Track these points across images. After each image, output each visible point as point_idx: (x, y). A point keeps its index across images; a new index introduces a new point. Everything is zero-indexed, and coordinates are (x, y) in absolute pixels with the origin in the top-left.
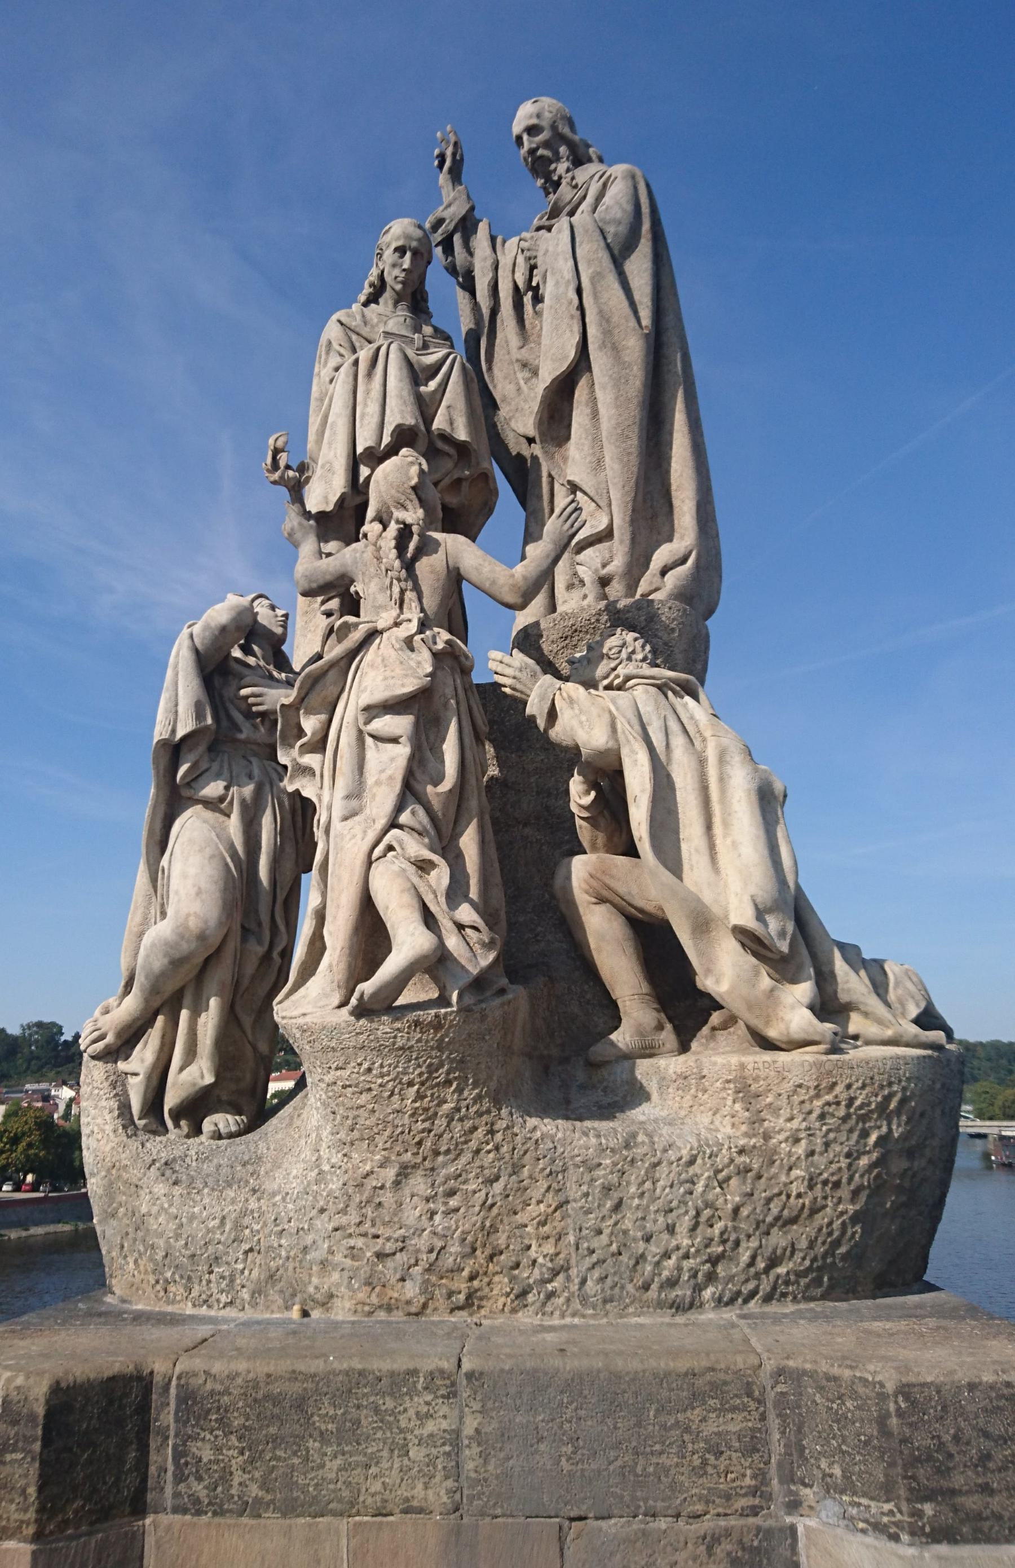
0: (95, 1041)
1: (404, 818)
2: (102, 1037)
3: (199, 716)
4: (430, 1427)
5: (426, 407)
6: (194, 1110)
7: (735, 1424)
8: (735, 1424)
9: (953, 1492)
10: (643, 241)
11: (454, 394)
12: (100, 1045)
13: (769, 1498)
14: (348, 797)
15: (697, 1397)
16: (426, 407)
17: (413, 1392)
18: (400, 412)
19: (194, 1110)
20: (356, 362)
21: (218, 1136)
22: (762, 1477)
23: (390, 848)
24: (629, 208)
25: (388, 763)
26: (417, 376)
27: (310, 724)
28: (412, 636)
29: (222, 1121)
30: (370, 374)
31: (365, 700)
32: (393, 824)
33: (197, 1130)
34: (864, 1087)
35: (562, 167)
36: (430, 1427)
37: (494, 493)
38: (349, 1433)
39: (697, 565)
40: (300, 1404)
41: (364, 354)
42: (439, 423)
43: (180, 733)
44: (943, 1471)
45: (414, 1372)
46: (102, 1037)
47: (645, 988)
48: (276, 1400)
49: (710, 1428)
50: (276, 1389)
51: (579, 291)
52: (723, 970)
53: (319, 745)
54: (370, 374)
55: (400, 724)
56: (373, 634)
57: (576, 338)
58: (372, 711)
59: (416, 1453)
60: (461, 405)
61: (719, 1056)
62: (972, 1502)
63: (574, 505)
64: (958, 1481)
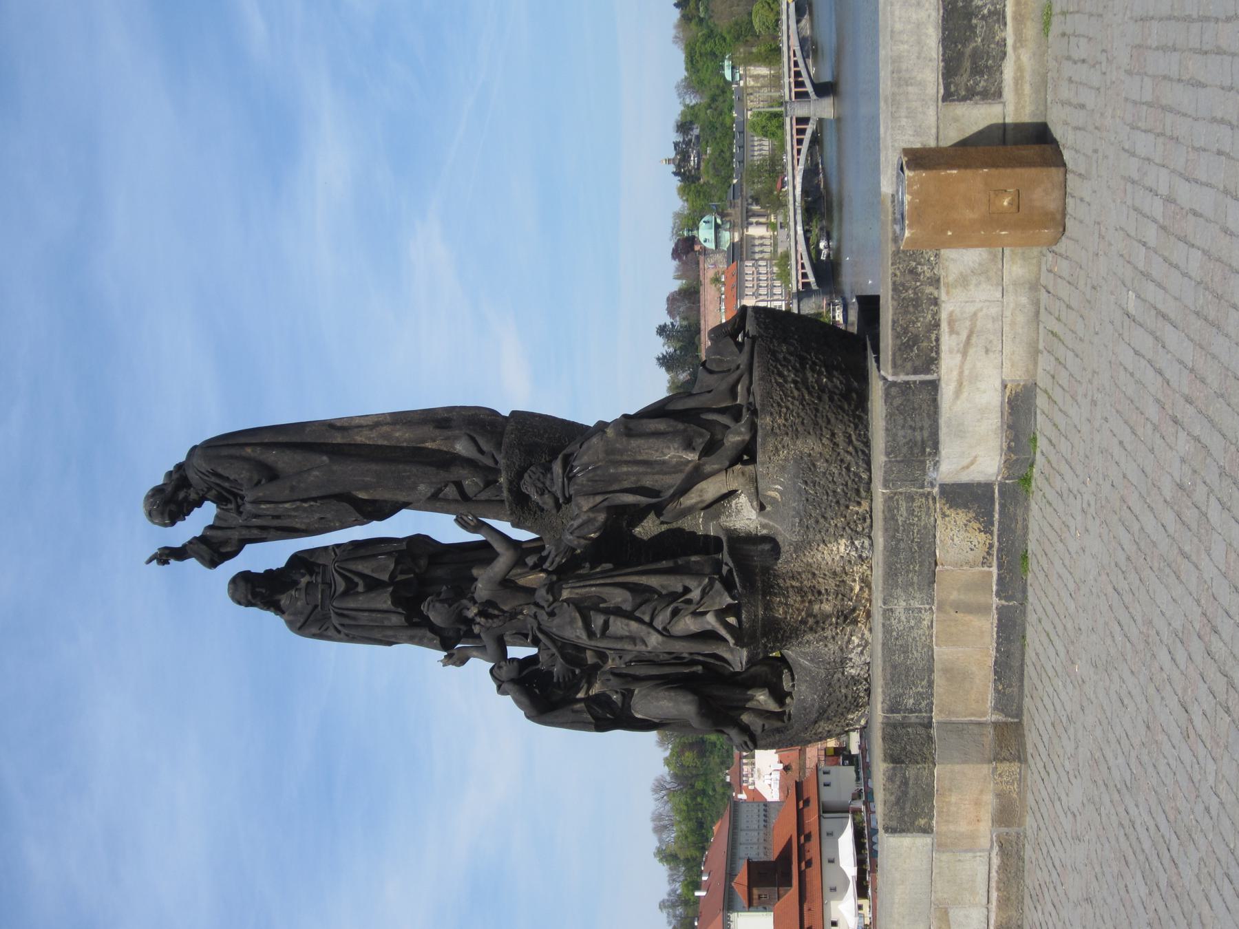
1: (647, 619)
4: (903, 618)
7: (903, 506)
8: (903, 506)
9: (923, 441)
13: (929, 493)
15: (893, 518)
16: (373, 585)
17: (891, 625)
19: (780, 696)
22: (922, 495)
25: (618, 626)
30: (354, 619)
31: (584, 636)
32: (650, 625)
36: (903, 618)
38: (905, 650)
40: (894, 667)
42: (385, 577)
44: (915, 444)
45: (884, 625)
46: (746, 743)
48: (893, 676)
49: (905, 514)
50: (889, 677)
54: (354, 619)
58: (591, 634)
59: (913, 623)
62: (926, 434)
64: (919, 438)
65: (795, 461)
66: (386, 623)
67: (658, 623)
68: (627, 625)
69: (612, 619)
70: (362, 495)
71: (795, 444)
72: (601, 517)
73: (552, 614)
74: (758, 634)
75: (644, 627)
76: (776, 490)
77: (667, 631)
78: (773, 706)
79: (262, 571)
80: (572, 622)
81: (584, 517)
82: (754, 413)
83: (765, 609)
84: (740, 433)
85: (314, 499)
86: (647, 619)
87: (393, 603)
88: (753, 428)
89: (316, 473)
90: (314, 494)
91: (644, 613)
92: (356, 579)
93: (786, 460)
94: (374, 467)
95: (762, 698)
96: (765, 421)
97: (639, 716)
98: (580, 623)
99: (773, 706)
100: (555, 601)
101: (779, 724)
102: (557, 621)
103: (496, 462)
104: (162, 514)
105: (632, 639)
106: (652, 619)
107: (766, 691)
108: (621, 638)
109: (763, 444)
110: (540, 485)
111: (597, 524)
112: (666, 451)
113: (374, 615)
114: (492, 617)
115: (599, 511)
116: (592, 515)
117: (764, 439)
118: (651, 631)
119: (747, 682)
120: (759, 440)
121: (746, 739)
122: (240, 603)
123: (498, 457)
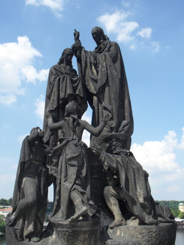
0: (9, 223)
1: (77, 182)
2: (10, 222)
3: (29, 156)
5: (75, 89)
6: (30, 237)
10: (118, 60)
11: (80, 86)
12: (10, 223)
14: (64, 177)
16: (75, 89)
18: (69, 91)
19: (30, 237)
20: (60, 79)
21: (35, 242)
23: (75, 189)
24: (116, 51)
26: (73, 82)
27: (55, 161)
28: (77, 143)
29: (35, 239)
30: (62, 82)
31: (68, 157)
32: (75, 183)
33: (30, 240)
34: (162, 231)
35: (102, 41)
37: (87, 107)
39: (130, 125)
41: (62, 77)
42: (77, 92)
43: (26, 160)
46: (10, 222)
47: (120, 213)
51: (107, 69)
52: (136, 210)
53: (57, 165)
54: (62, 82)
55: (75, 163)
56: (68, 142)
57: (106, 78)
58: (70, 159)
60: (82, 90)
61: (133, 223)
63: (108, 115)
65: (138, 241)
66: (60, 92)
67: (75, 186)
68: (74, 174)
69: (76, 168)
70: (107, 89)
71: (144, 241)
72: (114, 165)
73: (76, 145)
74: (74, 229)
75: (73, 181)
76: (121, 234)
77: (74, 190)
78: (26, 233)
79: (72, 61)
80: (74, 153)
81: (114, 159)
82: (157, 224)
83: (84, 231)
84: (149, 219)
85: (107, 72)
86: (77, 182)
87: (69, 94)
88: (151, 224)
89: (116, 73)
90: (108, 72)
91: (78, 181)
92: (76, 84)
93: (137, 237)
94: (118, 91)
95: (31, 228)
96: (154, 228)
97: (24, 179)
98: (74, 155)
99: (26, 233)
100: (81, 146)
101: (18, 236)
102: (73, 147)
103: (120, 132)
104: (97, 30)
105: (66, 176)
106: (77, 184)
107: (33, 230)
108: (66, 171)
109: (145, 228)
110: (117, 145)
111: (111, 164)
112: (142, 190)
113: (64, 88)
114: (73, 124)
115: (117, 165)
116: (115, 162)
117: (147, 228)
118: (72, 184)
119: (38, 222)
120: (146, 226)
121: (12, 222)
122: (65, 50)
123: (122, 132)
